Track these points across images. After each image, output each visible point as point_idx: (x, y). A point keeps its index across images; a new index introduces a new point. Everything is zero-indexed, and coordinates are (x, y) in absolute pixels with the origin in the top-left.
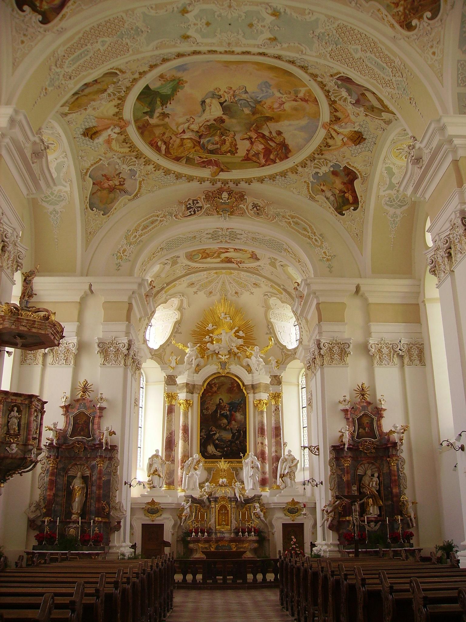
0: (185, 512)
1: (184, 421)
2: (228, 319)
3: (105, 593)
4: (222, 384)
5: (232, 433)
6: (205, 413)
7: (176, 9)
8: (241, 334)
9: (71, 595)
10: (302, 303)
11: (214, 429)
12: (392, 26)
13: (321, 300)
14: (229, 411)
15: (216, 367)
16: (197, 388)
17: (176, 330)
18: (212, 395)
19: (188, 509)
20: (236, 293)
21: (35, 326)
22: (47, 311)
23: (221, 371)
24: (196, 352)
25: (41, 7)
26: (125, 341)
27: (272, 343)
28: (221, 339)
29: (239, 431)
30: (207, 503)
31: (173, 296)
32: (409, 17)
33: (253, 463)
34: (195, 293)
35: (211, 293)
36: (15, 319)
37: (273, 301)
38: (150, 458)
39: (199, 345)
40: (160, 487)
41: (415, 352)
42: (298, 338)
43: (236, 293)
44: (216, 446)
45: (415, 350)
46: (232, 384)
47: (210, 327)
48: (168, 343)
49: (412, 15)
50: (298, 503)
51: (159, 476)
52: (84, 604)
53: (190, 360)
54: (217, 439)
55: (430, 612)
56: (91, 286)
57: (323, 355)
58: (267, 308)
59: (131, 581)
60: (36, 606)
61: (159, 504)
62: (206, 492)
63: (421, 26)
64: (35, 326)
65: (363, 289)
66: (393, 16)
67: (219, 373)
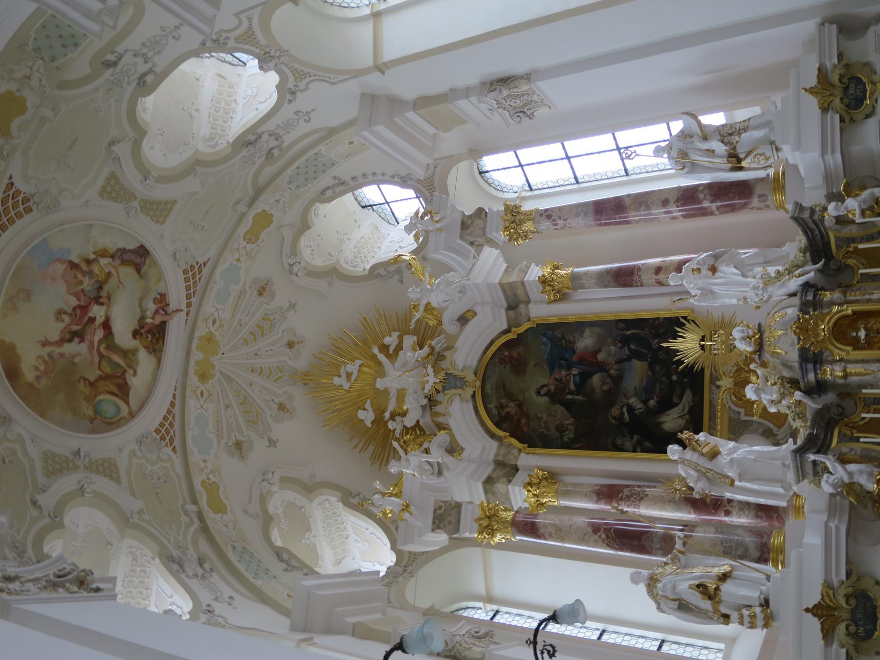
0: (863, 480)
1: (586, 496)
4: (504, 390)
5: (629, 359)
6: (572, 436)
11: (615, 411)
14: (569, 368)
15: (457, 402)
16: (505, 455)
18: (528, 416)
19: (852, 467)
20: (291, 345)
23: (469, 391)
29: (625, 341)
30: (830, 397)
33: (699, 270)
35: (282, 407)
38: (659, 608)
40: (768, 578)
43: (291, 345)
44: (666, 405)
46: (502, 361)
47: (367, 416)
50: (822, 73)
51: (724, 577)
53: (428, 467)
54: (645, 402)
61: (828, 585)
62: (783, 396)
67: (473, 396)
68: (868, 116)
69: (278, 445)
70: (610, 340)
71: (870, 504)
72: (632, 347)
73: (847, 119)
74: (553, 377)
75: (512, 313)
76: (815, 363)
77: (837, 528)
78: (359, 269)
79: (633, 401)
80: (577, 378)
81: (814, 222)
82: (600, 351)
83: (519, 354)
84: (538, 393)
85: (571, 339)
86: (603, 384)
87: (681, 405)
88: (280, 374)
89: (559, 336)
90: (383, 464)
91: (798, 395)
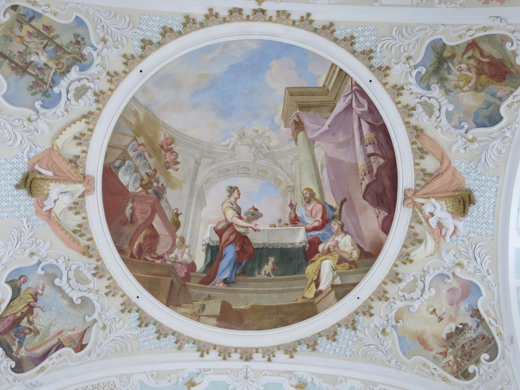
7: (181, 380)
12: (445, 379)
25: (17, 353)
32: (463, 364)
49: (466, 362)
63: (481, 370)
66: (443, 367)
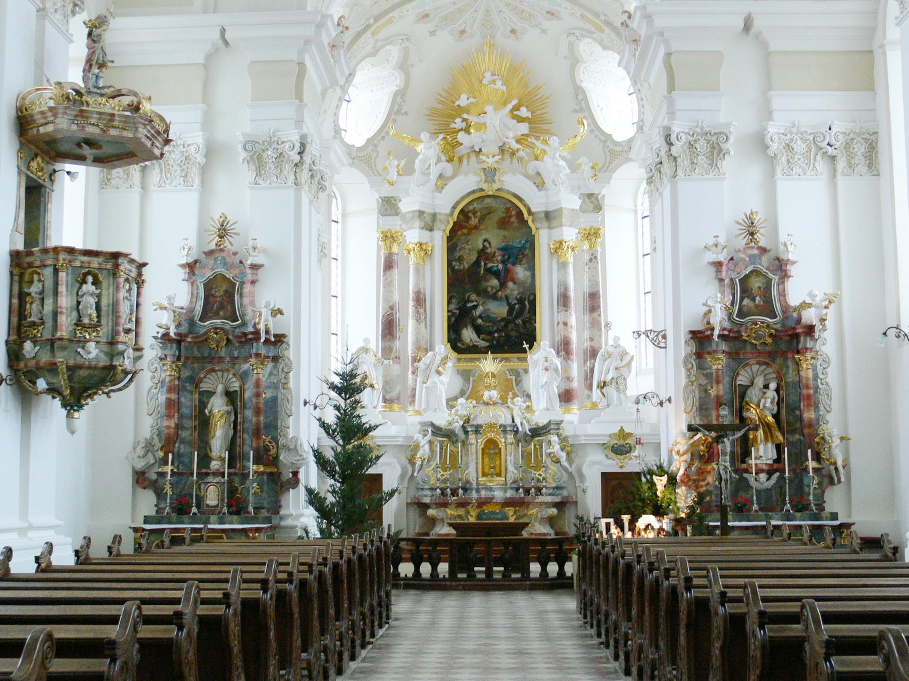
1: (417, 284)
2: (499, 83)
3: (243, 599)
4: (489, 212)
5: (509, 304)
6: (456, 267)
8: (524, 112)
9: (176, 601)
10: (637, 53)
11: (473, 297)
13: (675, 46)
14: (503, 262)
16: (441, 221)
17: (396, 107)
18: (469, 234)
19: (427, 447)
21: (115, 123)
22: (135, 94)
23: (485, 186)
24: (438, 151)
26: (295, 138)
27: (583, 131)
28: (484, 124)
29: (521, 301)
30: (462, 436)
31: (389, 41)
33: (547, 361)
34: (433, 33)
35: (463, 32)
36: (75, 113)
37: (586, 47)
39: (441, 136)
40: (375, 407)
41: (860, 149)
42: (636, 120)
43: (513, 31)
44: (478, 330)
45: (859, 144)
46: (508, 210)
47: (463, 101)
48: (383, 134)
50: (630, 435)
52: (199, 616)
53: (426, 167)
54: (480, 317)
55: (769, 637)
56: (223, 32)
57: (675, 158)
58: (574, 61)
59: (294, 578)
60: (112, 620)
62: (460, 416)
64: (115, 123)
65: (758, 23)
67: (482, 190)
68: (606, 456)
69: (432, 37)
70: (522, 290)
71: (413, 453)
72: (517, 306)
73: (606, 446)
74: (497, 251)
75: (542, 215)
76: (476, 431)
77: (398, 441)
78: (581, 75)
79: (481, 308)
80: (495, 269)
81: (549, 431)
82: (515, 283)
83: (513, 222)
84: (485, 240)
85: (523, 262)
86: (492, 287)
87: (478, 340)
88: (488, 27)
89: (526, 253)
90: (429, 117)
91: (462, 423)
